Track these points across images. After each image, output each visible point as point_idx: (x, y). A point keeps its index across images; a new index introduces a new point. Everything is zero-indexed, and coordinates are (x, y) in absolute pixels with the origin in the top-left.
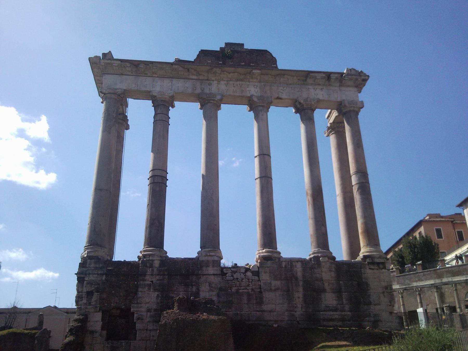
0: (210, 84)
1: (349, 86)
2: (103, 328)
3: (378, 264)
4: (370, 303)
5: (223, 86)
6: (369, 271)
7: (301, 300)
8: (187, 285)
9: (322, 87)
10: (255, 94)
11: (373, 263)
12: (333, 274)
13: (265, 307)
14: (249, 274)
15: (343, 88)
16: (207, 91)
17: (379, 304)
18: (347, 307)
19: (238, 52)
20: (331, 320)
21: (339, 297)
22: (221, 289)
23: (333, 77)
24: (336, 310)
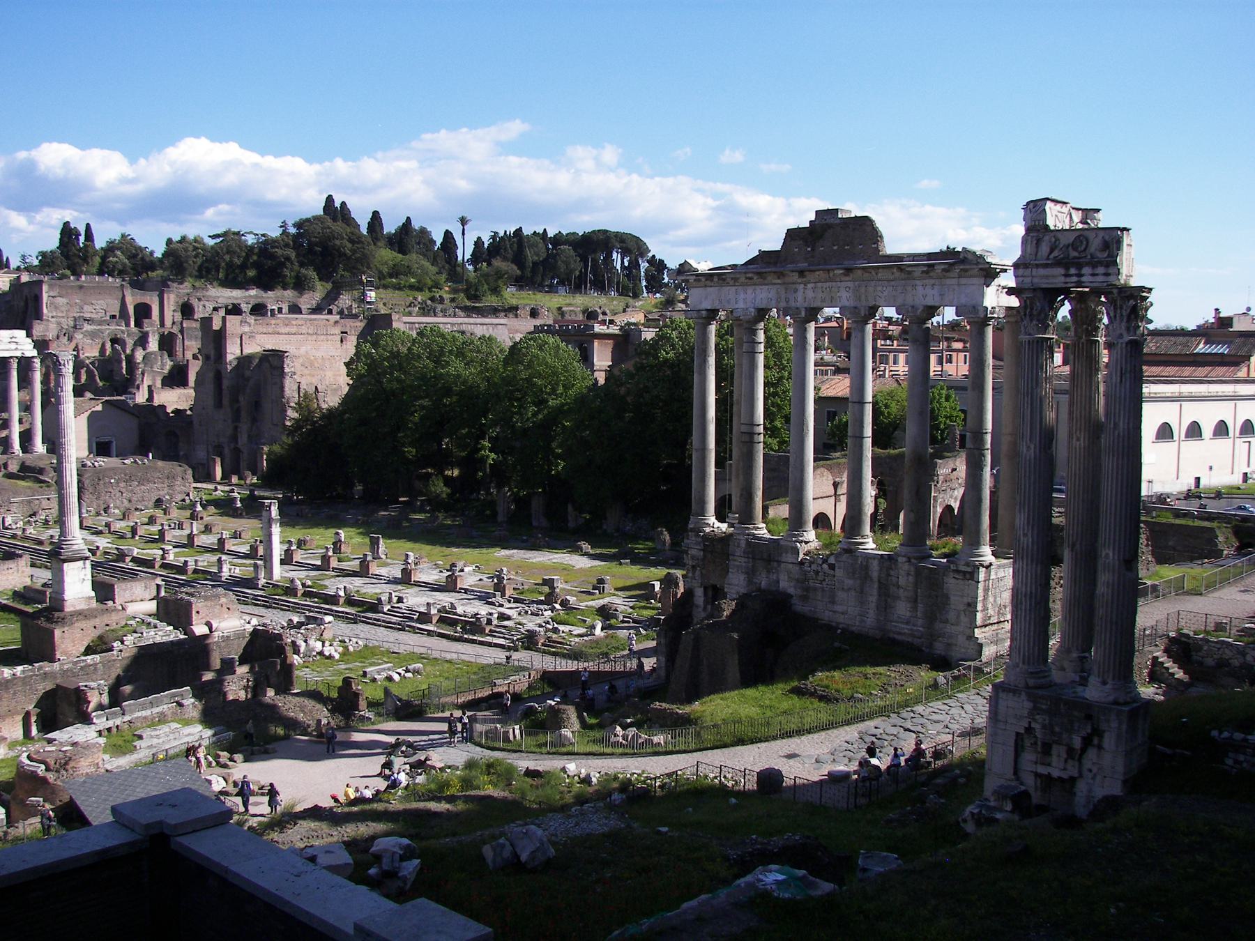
0: (796, 291)
1: (971, 276)
2: (706, 602)
3: (965, 573)
4: (946, 621)
5: (810, 294)
6: (953, 581)
7: (873, 605)
8: (768, 572)
9: (932, 281)
10: (847, 304)
11: (958, 571)
12: (911, 579)
13: (839, 608)
14: (825, 566)
15: (963, 281)
16: (792, 304)
17: (957, 624)
18: (920, 622)
19: (830, 226)
20: (900, 633)
21: (915, 608)
22: (798, 580)
23: (939, 269)
24: (907, 623)
